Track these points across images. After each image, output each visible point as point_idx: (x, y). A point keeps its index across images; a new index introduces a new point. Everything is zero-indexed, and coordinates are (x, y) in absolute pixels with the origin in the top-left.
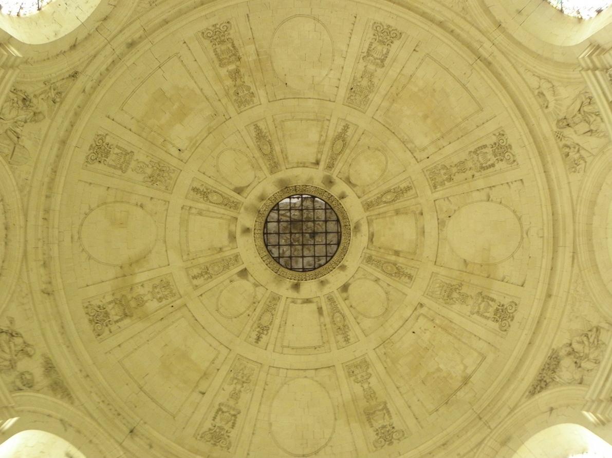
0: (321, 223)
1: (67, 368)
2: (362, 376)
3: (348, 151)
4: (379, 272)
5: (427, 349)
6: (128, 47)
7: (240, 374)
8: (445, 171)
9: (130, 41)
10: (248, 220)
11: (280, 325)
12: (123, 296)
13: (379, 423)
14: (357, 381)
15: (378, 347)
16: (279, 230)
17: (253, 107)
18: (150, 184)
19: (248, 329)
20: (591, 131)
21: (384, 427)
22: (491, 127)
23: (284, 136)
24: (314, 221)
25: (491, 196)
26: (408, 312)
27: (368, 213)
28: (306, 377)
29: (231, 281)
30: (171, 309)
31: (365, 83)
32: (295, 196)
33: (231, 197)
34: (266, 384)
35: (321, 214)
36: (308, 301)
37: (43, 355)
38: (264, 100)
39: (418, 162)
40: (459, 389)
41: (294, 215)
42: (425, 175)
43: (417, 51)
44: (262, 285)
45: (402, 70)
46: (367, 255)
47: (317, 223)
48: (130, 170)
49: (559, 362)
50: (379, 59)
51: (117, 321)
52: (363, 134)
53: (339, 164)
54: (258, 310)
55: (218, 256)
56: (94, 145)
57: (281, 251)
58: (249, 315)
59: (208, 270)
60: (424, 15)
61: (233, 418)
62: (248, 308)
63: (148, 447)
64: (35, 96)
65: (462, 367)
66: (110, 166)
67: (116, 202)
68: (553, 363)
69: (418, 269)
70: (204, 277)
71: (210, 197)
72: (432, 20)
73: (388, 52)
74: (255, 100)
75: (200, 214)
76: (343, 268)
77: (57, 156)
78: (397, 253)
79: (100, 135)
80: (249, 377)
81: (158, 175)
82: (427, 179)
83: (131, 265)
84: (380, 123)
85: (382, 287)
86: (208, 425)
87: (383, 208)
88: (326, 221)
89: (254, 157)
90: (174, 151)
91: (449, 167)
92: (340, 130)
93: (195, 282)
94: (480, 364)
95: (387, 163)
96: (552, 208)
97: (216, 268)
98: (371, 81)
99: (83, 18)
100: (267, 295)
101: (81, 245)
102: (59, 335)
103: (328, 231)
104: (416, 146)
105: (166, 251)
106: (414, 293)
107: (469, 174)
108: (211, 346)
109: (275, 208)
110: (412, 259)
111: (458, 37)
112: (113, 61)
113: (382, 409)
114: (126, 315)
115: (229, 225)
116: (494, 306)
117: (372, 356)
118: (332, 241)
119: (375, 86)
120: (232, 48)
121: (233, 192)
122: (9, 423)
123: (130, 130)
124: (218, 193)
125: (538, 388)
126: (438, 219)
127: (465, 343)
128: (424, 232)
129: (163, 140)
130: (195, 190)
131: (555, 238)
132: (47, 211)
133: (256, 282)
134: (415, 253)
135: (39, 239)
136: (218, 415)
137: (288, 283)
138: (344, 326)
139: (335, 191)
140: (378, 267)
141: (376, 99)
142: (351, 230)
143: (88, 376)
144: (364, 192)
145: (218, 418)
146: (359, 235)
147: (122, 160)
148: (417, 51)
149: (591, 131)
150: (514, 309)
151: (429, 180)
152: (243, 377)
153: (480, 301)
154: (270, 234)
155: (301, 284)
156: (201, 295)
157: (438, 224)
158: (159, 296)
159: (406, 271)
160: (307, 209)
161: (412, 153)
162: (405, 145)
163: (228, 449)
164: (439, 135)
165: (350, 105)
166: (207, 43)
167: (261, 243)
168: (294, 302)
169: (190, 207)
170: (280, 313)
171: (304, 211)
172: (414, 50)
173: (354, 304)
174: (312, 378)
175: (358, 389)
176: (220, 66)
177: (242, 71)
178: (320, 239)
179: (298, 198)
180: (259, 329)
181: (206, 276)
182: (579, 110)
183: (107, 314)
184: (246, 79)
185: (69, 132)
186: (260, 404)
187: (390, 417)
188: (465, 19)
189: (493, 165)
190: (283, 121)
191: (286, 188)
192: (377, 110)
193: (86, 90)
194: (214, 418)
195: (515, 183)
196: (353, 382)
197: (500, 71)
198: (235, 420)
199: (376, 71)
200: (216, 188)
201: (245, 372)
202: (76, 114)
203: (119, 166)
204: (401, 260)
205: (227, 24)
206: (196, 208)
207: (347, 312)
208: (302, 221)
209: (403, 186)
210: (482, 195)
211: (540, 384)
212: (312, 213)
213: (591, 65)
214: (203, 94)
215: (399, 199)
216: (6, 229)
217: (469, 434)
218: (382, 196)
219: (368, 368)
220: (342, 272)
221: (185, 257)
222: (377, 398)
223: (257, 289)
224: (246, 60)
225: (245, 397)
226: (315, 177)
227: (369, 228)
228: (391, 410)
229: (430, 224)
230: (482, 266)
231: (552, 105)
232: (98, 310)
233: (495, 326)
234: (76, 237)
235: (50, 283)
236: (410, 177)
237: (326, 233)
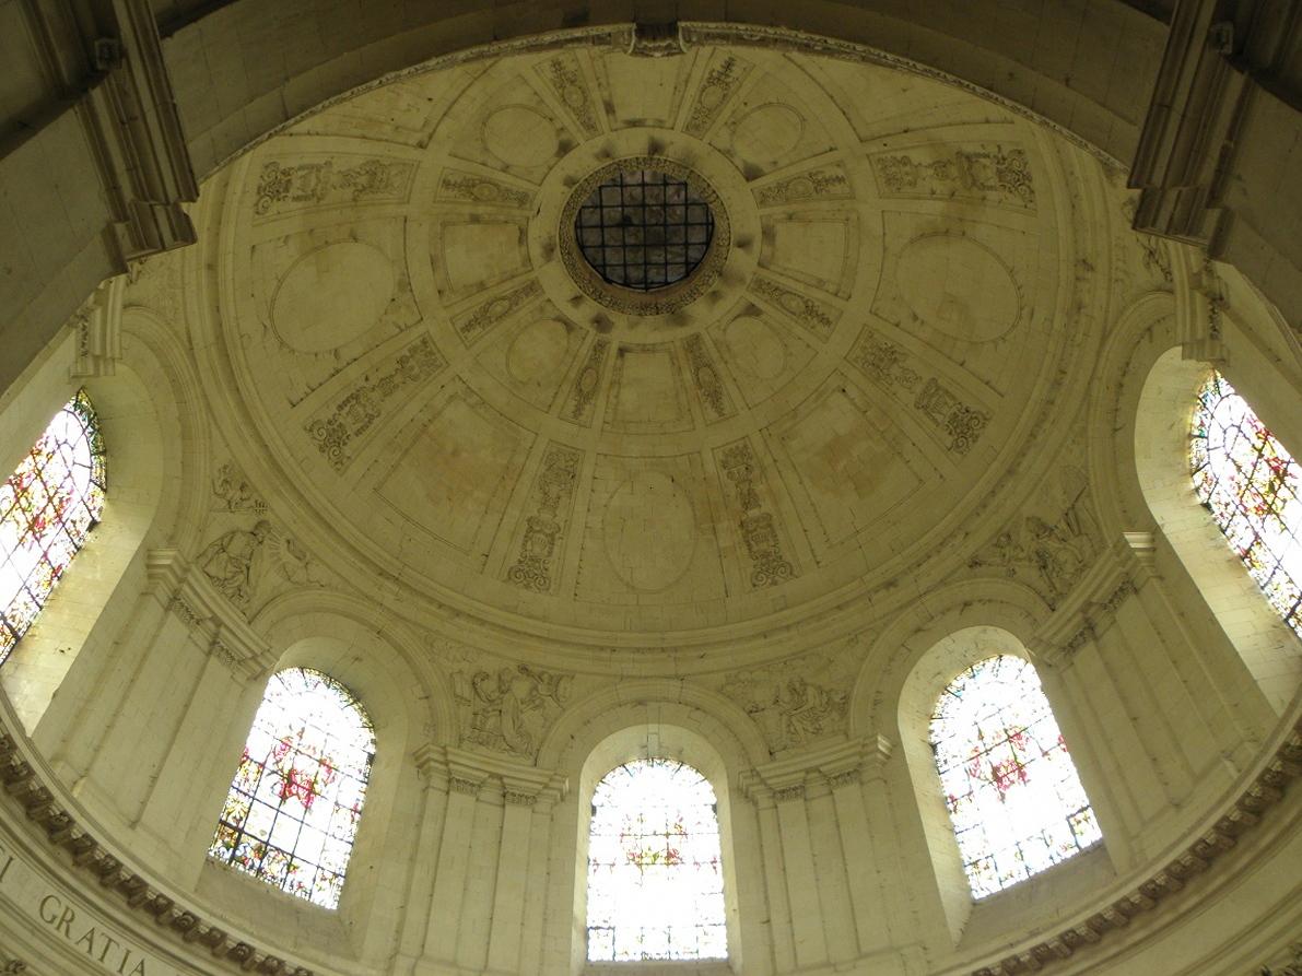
0: (612, 243)
3: (572, 375)
4: (503, 182)
6: (896, 580)
9: (892, 589)
10: (740, 261)
11: (686, 86)
17: (723, 446)
18: (896, 348)
23: (677, 395)
24: (624, 246)
27: (532, 276)
31: (554, 490)
33: (766, 301)
35: (613, 257)
41: (660, 256)
42: (443, 357)
44: (719, 151)
45: (501, 520)
46: (528, 206)
48: (924, 381)
51: (987, 156)
53: (585, 352)
54: (726, 113)
57: (683, 193)
59: (815, 188)
62: (746, 115)
66: (953, 398)
69: (434, 202)
73: (524, 545)
74: (720, 456)
76: (570, 182)
78: (475, 219)
81: (882, 360)
82: (439, 351)
83: (947, 231)
88: (603, 246)
89: (726, 363)
92: (587, 407)
93: (840, 172)
95: (507, 365)
96: (241, 398)
97: (801, 188)
99: (946, 641)
103: (599, 230)
104: (465, 400)
106: (436, 162)
107: (374, 380)
109: (692, 266)
111: (431, 600)
112: (919, 565)
114: (968, 158)
115: (773, 254)
116: (294, 192)
118: (592, 213)
120: (752, 543)
121: (763, 309)
124: (788, 310)
126: (411, 290)
129: (868, 413)
130: (825, 321)
132: (1057, 383)
134: (444, 225)
135: (1079, 345)
137: (671, 153)
138: (562, 87)
139: (590, 308)
142: (558, 247)
144: (542, 310)
150: (260, 205)
151: (435, 351)
153: (319, 188)
154: (701, 224)
155: (647, 151)
156: (831, 150)
158: (907, 168)
160: (637, 265)
161: (469, 388)
164: (431, 428)
165: (574, 451)
166: (788, 557)
167: (720, 224)
168: (660, 124)
169: (836, 295)
171: (641, 261)
173: (546, 123)
176: (771, 516)
177: (738, 505)
178: (614, 215)
179: (652, 283)
182: (248, 569)
185: (1000, 484)
189: (340, 407)
197: (363, 566)
199: (538, 511)
203: (941, 392)
204: (467, 210)
205: (757, 583)
206: (827, 291)
207: (559, 111)
208: (645, 246)
210: (346, 355)
213: (260, 659)
214: (798, 474)
216: (1121, 385)
220: (572, 173)
221: (854, 216)
224: (732, 522)
226: (627, 331)
229: (423, 280)
231: (283, 546)
234: (1025, 312)
235: (1077, 279)
236: (467, 348)
237: (602, 227)
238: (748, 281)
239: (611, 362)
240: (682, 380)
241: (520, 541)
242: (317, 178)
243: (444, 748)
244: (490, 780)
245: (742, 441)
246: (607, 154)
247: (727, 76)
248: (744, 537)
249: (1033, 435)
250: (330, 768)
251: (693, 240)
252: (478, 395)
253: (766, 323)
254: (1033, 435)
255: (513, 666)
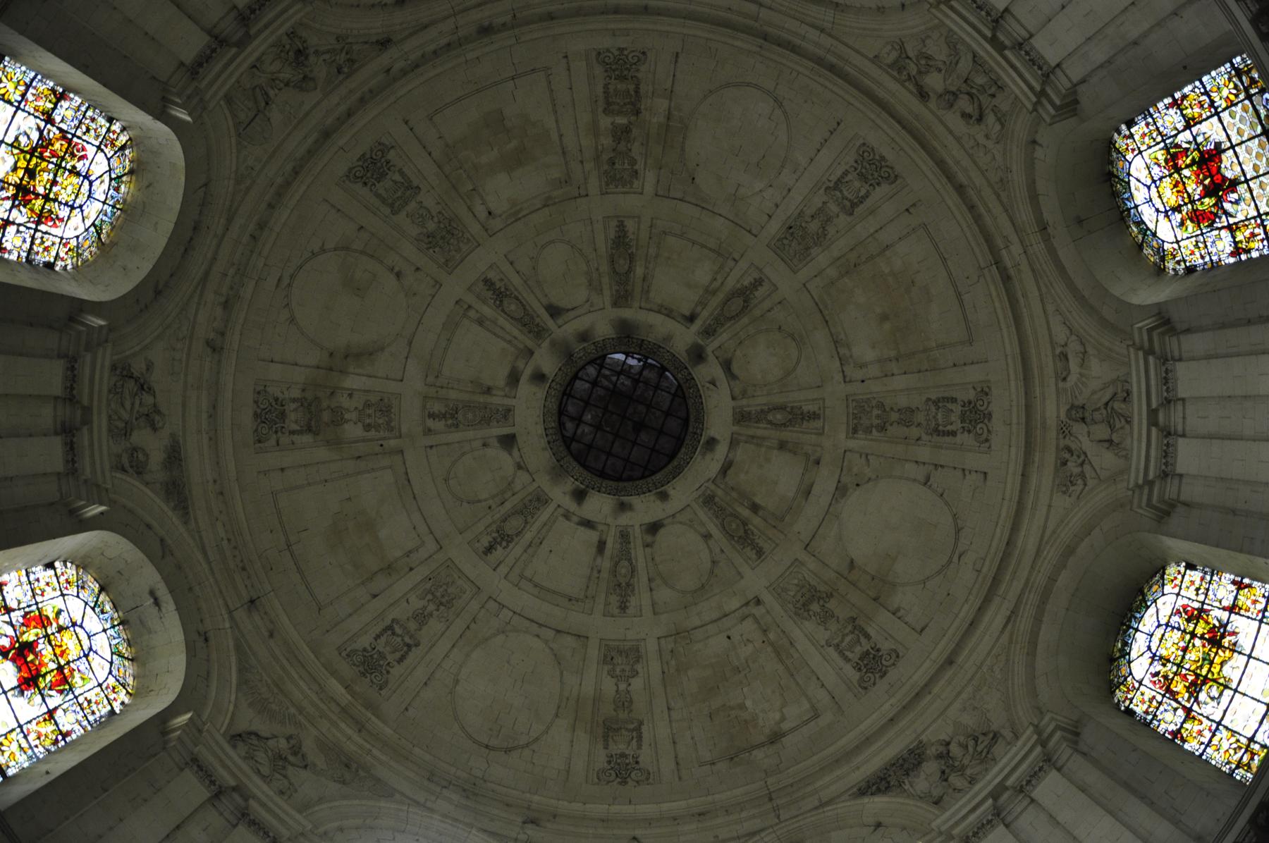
0: (658, 413)
1: (198, 468)
2: (623, 670)
3: (745, 320)
4: (716, 526)
5: (737, 670)
7: (441, 590)
8: (880, 412)
9: (486, 23)
10: (547, 362)
11: (531, 542)
12: (317, 398)
13: (619, 747)
14: (611, 674)
15: (665, 637)
16: (589, 398)
18: (426, 246)
19: (481, 527)
20: (1110, 441)
21: (623, 755)
22: (974, 375)
23: (657, 256)
25: (932, 479)
26: (735, 603)
27: (736, 428)
28: (538, 636)
29: (485, 445)
30: (378, 449)
31: (814, 226)
32: (635, 356)
33: (538, 316)
34: (474, 620)
36: (588, 524)
37: (173, 435)
38: (649, 188)
39: (845, 382)
40: (762, 745)
43: (910, 213)
44: (528, 471)
45: (877, 231)
47: (653, 410)
48: (405, 213)
49: (920, 763)
50: (850, 200)
51: (293, 432)
52: (780, 303)
54: (508, 505)
55: (481, 399)
56: (368, 156)
57: (579, 431)
58: (490, 508)
59: (457, 413)
60: (941, 164)
61: (405, 649)
63: (266, 634)
64: (316, 52)
65: (778, 716)
66: (378, 195)
67: (362, 252)
68: (910, 762)
69: (777, 545)
70: (446, 421)
71: (505, 303)
72: (950, 177)
73: (867, 195)
74: (636, 184)
75: (480, 322)
76: (664, 496)
77: (309, 152)
78: (755, 508)
79: (383, 144)
80: (453, 599)
81: (443, 238)
82: (848, 414)
83: (346, 357)
84: (813, 297)
85: (711, 551)
86: (365, 641)
87: (761, 430)
88: (668, 414)
89: (597, 269)
90: (481, 211)
91: (887, 410)
92: (746, 283)
93: (430, 423)
94: (806, 723)
95: (798, 362)
96: (1011, 535)
97: (470, 416)
98: (824, 228)
100: (531, 488)
101: (287, 296)
102: (204, 416)
104: (851, 356)
105: (407, 358)
106: (755, 580)
107: (915, 432)
108: (414, 528)
109: (598, 362)
110: (774, 527)
111: (978, 219)
113: (633, 730)
114: (309, 429)
116: (866, 645)
117: (651, 646)
119: (828, 237)
120: (633, 93)
122: (96, 510)
123: (430, 154)
124: (521, 302)
125: (874, 788)
126: (839, 482)
127: (797, 684)
128: (809, 493)
129: (471, 188)
130: (488, 283)
131: (996, 581)
132: (262, 226)
133: (522, 463)
134: (782, 519)
136: (385, 635)
137: (569, 484)
138: (628, 585)
140: (717, 517)
141: (821, 258)
142: (701, 443)
143: (222, 493)
145: (383, 639)
146: (709, 457)
147: (399, 194)
148: (910, 213)
149: (1110, 441)
150: (892, 661)
152: (443, 596)
153: (847, 631)
156: (431, 447)
157: (837, 488)
158: (368, 421)
159: (756, 541)
162: (837, 347)
163: (381, 689)
164: (893, 353)
166: (599, 70)
167: (553, 405)
168: (567, 516)
169: (470, 307)
170: (538, 524)
171: (641, 384)
172: (907, 210)
174: (546, 642)
175: (609, 686)
176: (604, 112)
177: (635, 132)
179: (639, 360)
180: (495, 535)
181: (450, 422)
182: (1107, 404)
183: (283, 415)
184: (636, 149)
186: (453, 646)
187: (639, 747)
188: (998, 196)
189: (953, 434)
190: (665, 233)
191: (627, 336)
192: (816, 276)
193: (391, 72)
194: (377, 637)
195: (974, 474)
196: (605, 672)
197: (1019, 294)
198: (407, 653)
199: (838, 216)
200: (519, 293)
201: (449, 591)
202: (362, 100)
203: (390, 201)
204: (756, 520)
206: (477, 311)
207: (641, 564)
209: (808, 408)
211: (879, 784)
212: (651, 393)
213: (1146, 345)
215: (794, 427)
216: (195, 228)
217: (744, 814)
218: (770, 410)
219: (638, 661)
220: (658, 502)
221: (431, 379)
222: (631, 711)
223: (520, 473)
225: (434, 626)
226: (682, 338)
227: (729, 451)
228: (645, 735)
229: (825, 483)
230: (873, 579)
231: (1073, 379)
232: (274, 403)
233: (854, 676)
234: (286, 281)
235: (223, 334)
238: (548, 341)
239: (705, 314)
240: (646, 268)
241: (868, 202)
242: (842, 641)
243: (1035, 110)
244: (1007, 43)
245: (608, 191)
246: (623, 507)
247: (494, 539)
248: (639, 101)
249: (296, 172)
250: (1174, 157)
251: (587, 385)
252: (838, 353)
253: (546, 296)
254: (296, 172)
255: (932, 104)
